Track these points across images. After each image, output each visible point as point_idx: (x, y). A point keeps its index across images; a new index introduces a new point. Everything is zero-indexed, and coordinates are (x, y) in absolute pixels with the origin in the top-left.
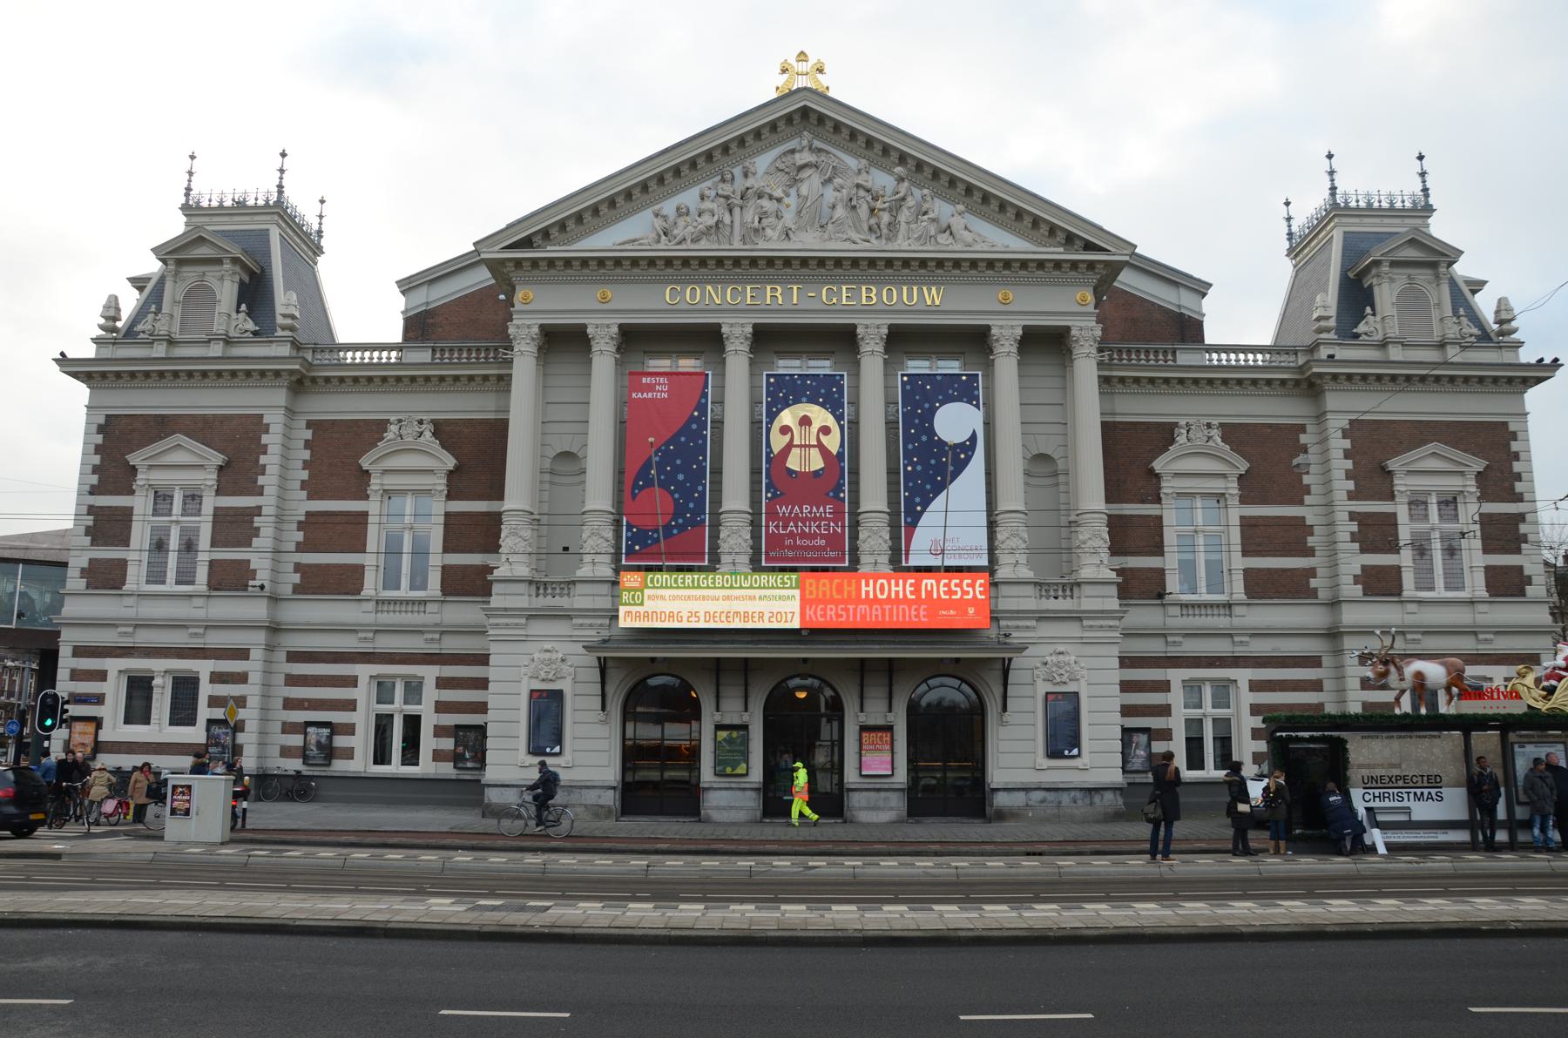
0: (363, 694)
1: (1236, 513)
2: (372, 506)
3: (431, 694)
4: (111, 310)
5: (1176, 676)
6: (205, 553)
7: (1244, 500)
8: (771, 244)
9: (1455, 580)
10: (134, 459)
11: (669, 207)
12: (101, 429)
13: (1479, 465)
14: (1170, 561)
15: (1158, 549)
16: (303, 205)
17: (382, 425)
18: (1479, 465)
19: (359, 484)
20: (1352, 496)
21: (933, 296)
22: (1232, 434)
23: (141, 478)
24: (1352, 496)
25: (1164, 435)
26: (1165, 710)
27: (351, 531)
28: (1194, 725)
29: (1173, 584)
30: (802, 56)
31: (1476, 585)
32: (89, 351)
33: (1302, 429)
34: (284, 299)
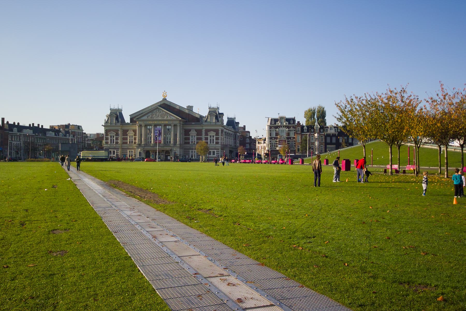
0: (128, 152)
1: (196, 137)
2: (128, 137)
3: (133, 152)
4: (105, 120)
5: (190, 150)
6: (115, 141)
7: (197, 136)
8: (155, 118)
9: (213, 143)
10: (108, 133)
11: (148, 115)
12: (105, 131)
13: (215, 133)
14: (190, 141)
15: (189, 140)
16: (120, 108)
17: (128, 130)
18: (215, 133)
19: (127, 135)
20: (205, 136)
21: (167, 122)
22: (196, 130)
23: (109, 135)
24: (205, 136)
25: (190, 130)
26: (189, 153)
27: (127, 139)
28: (192, 154)
29: (191, 143)
30: (165, 91)
31: (215, 143)
32: (104, 124)
33: (202, 130)
34: (120, 120)
